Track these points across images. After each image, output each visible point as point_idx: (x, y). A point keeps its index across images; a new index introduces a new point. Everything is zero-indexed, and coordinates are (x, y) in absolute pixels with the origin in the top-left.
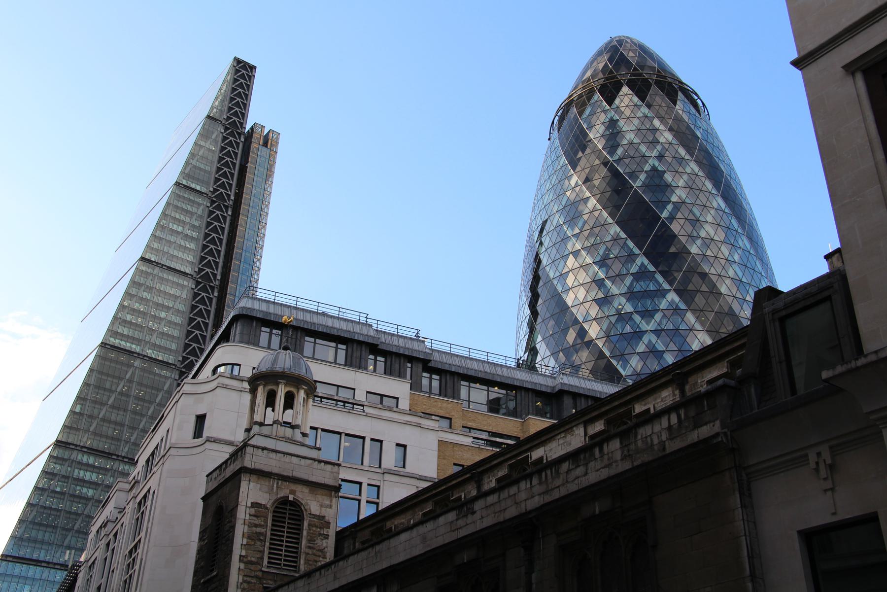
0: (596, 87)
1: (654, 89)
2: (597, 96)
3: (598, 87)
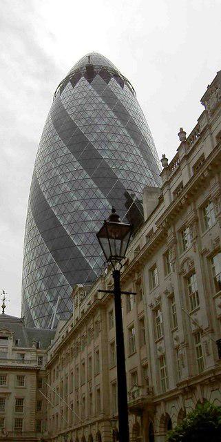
1: (113, 79)
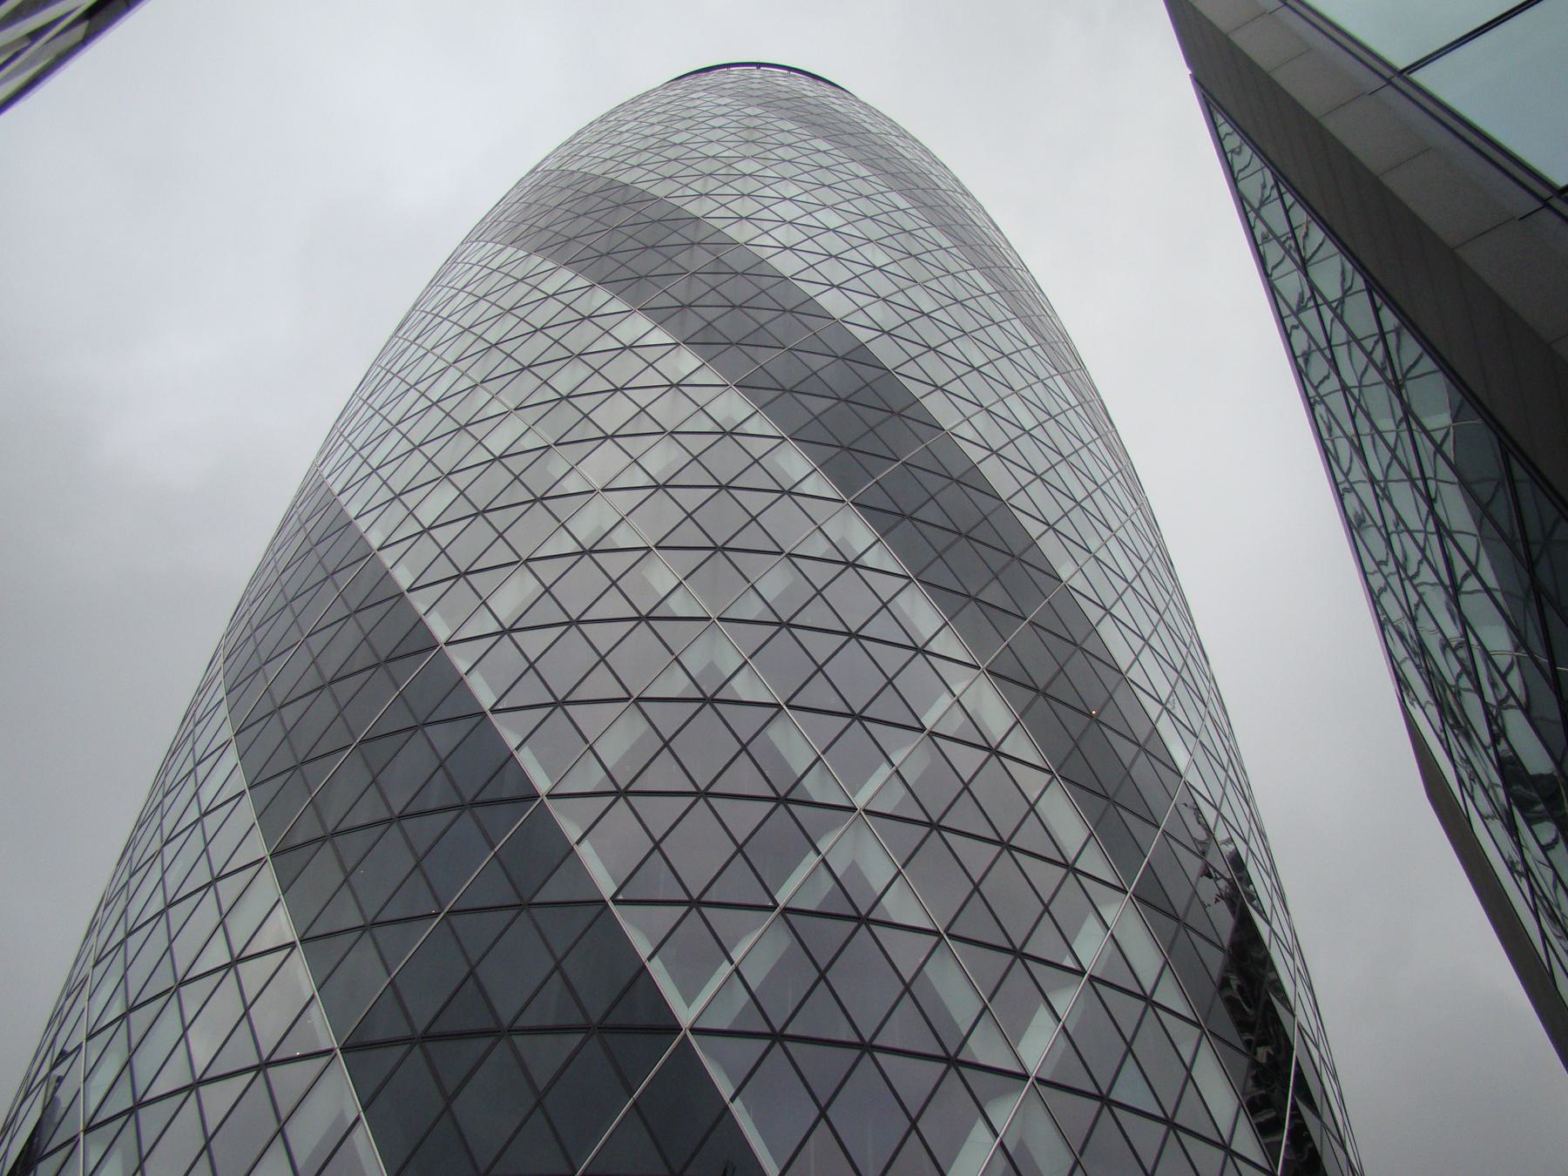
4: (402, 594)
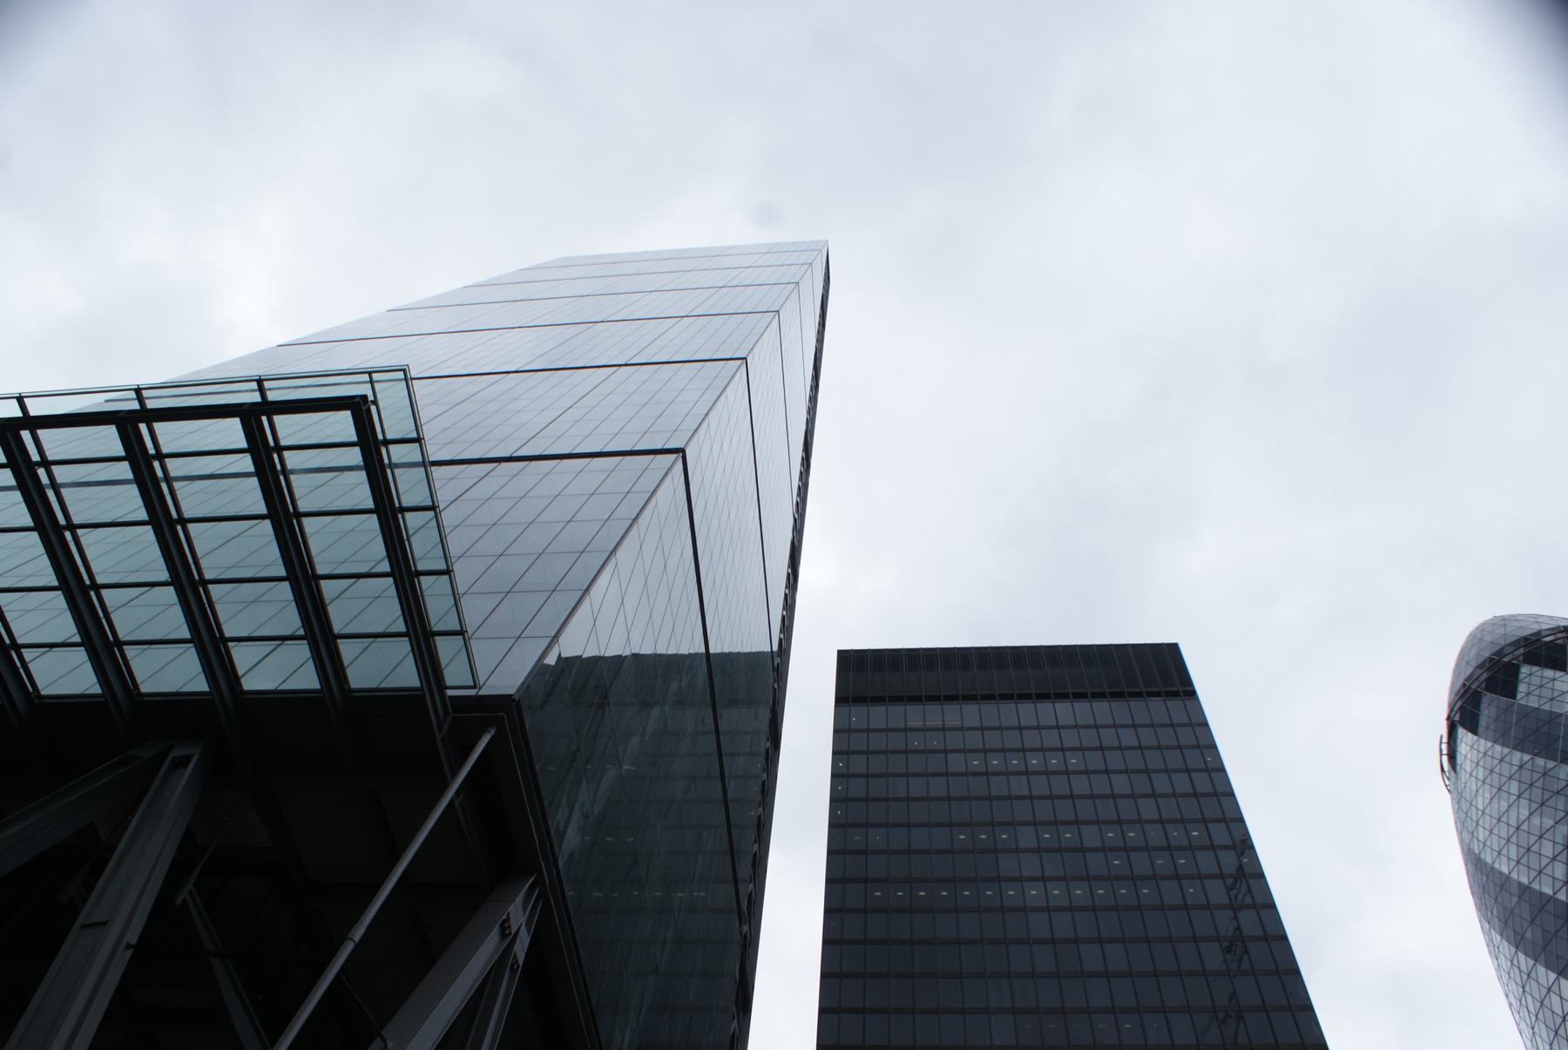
0: (1478, 687)
2: (1487, 698)
3: (1483, 686)
4: (1528, 887)
